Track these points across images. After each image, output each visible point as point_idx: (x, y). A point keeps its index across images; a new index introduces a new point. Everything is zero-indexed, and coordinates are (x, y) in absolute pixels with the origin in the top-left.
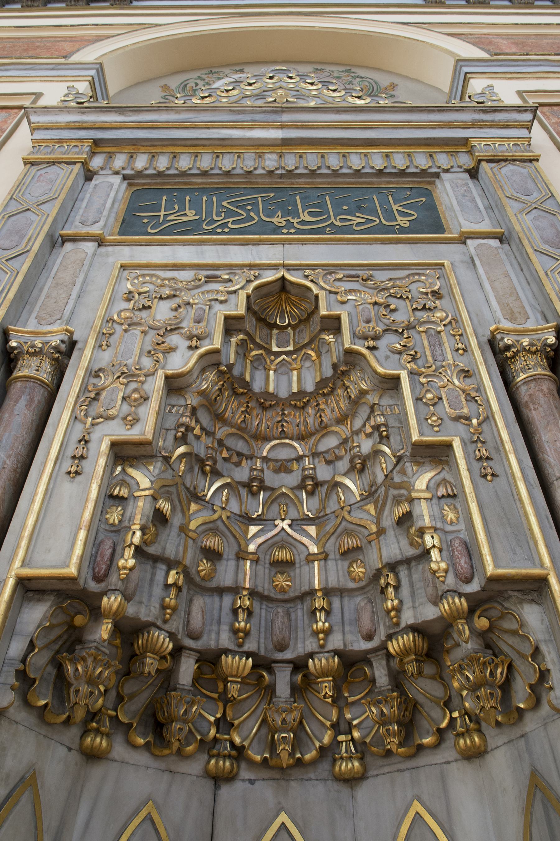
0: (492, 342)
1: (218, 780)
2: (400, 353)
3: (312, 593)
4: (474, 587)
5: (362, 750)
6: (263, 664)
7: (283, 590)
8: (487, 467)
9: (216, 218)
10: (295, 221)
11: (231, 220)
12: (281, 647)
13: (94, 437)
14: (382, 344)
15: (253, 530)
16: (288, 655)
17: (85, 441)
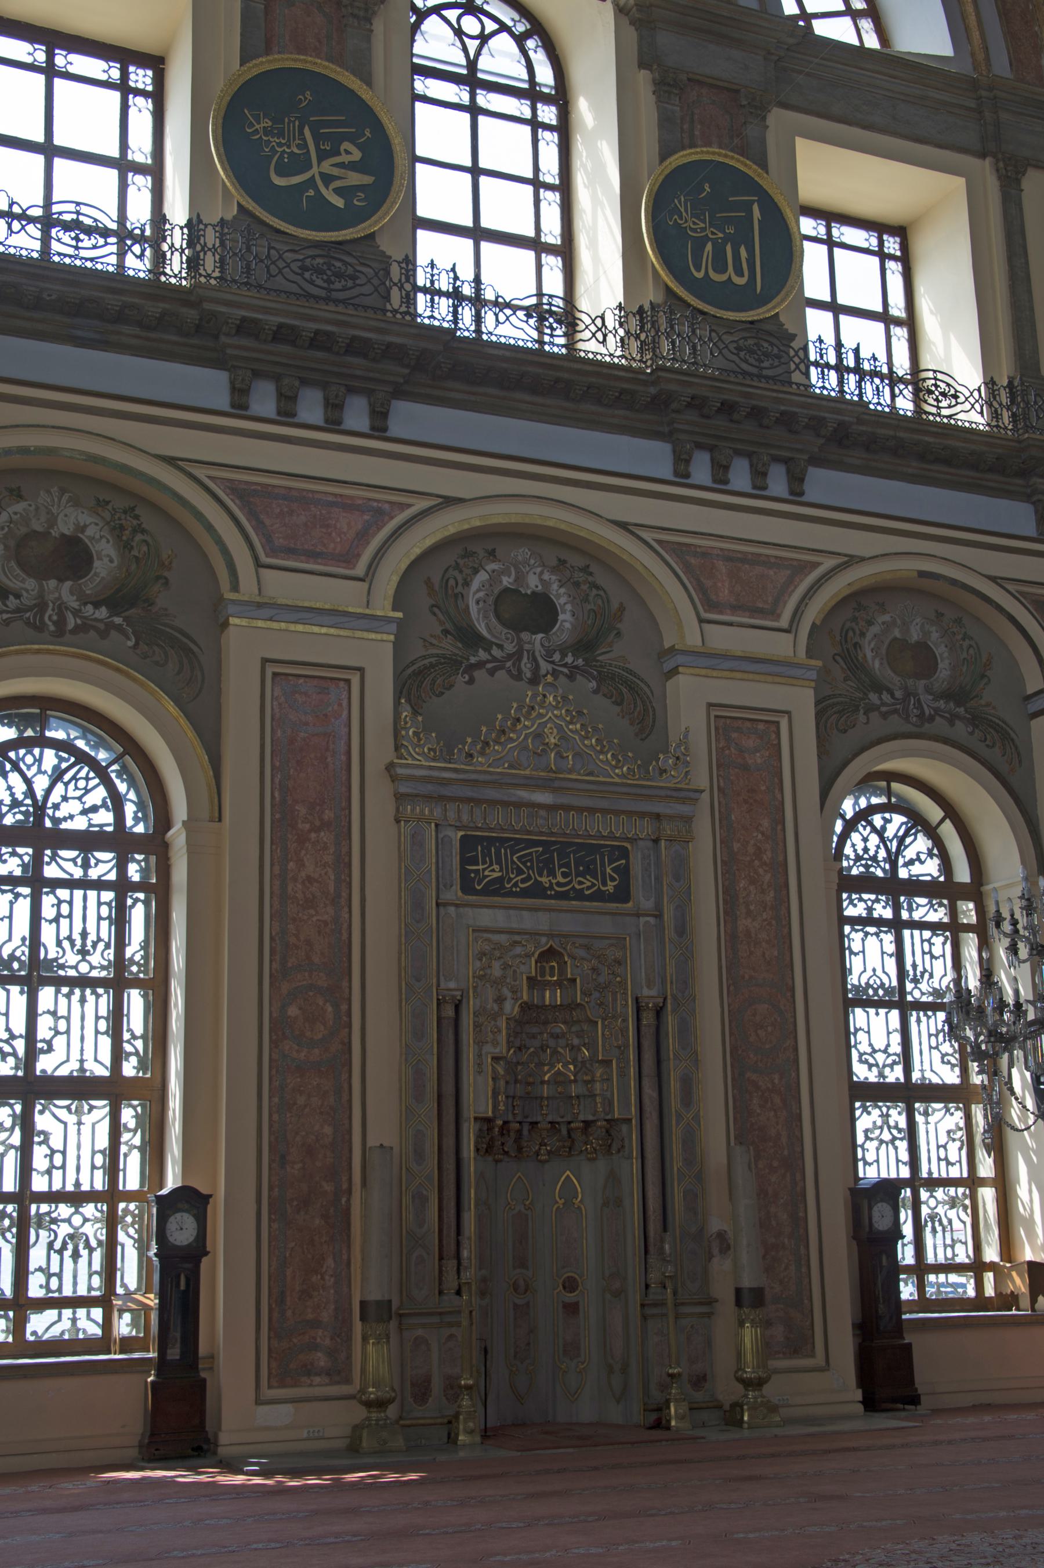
0: (637, 999)
1: (497, 1161)
2: (600, 1005)
3: (542, 1098)
4: (609, 1117)
5: (549, 1153)
6: (520, 1123)
7: (528, 1093)
8: (623, 1074)
9: (512, 876)
10: (554, 881)
11: (519, 878)
12: (527, 1117)
13: (483, 1052)
14: (593, 997)
15: (519, 1068)
16: (529, 1120)
17: (480, 1056)
